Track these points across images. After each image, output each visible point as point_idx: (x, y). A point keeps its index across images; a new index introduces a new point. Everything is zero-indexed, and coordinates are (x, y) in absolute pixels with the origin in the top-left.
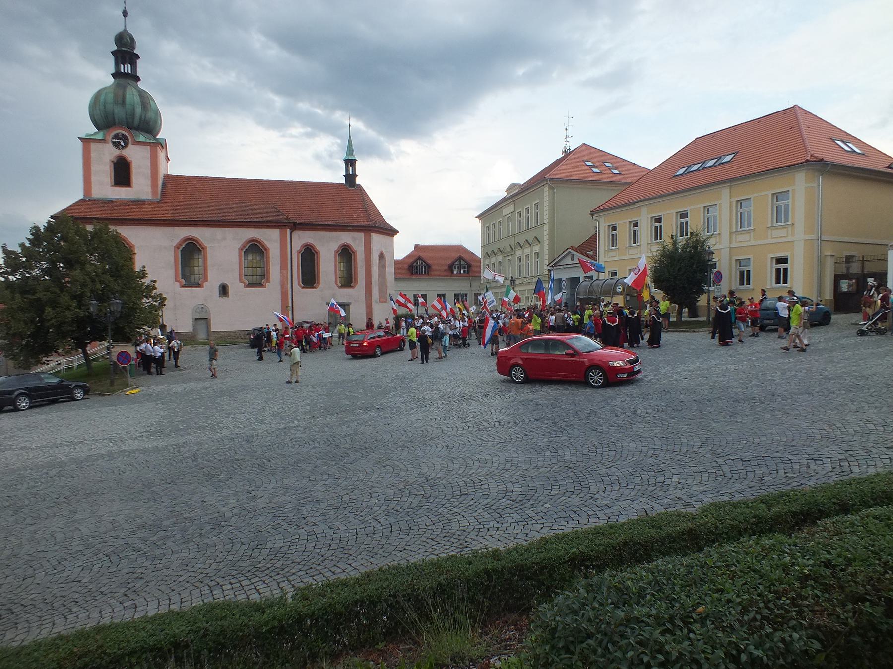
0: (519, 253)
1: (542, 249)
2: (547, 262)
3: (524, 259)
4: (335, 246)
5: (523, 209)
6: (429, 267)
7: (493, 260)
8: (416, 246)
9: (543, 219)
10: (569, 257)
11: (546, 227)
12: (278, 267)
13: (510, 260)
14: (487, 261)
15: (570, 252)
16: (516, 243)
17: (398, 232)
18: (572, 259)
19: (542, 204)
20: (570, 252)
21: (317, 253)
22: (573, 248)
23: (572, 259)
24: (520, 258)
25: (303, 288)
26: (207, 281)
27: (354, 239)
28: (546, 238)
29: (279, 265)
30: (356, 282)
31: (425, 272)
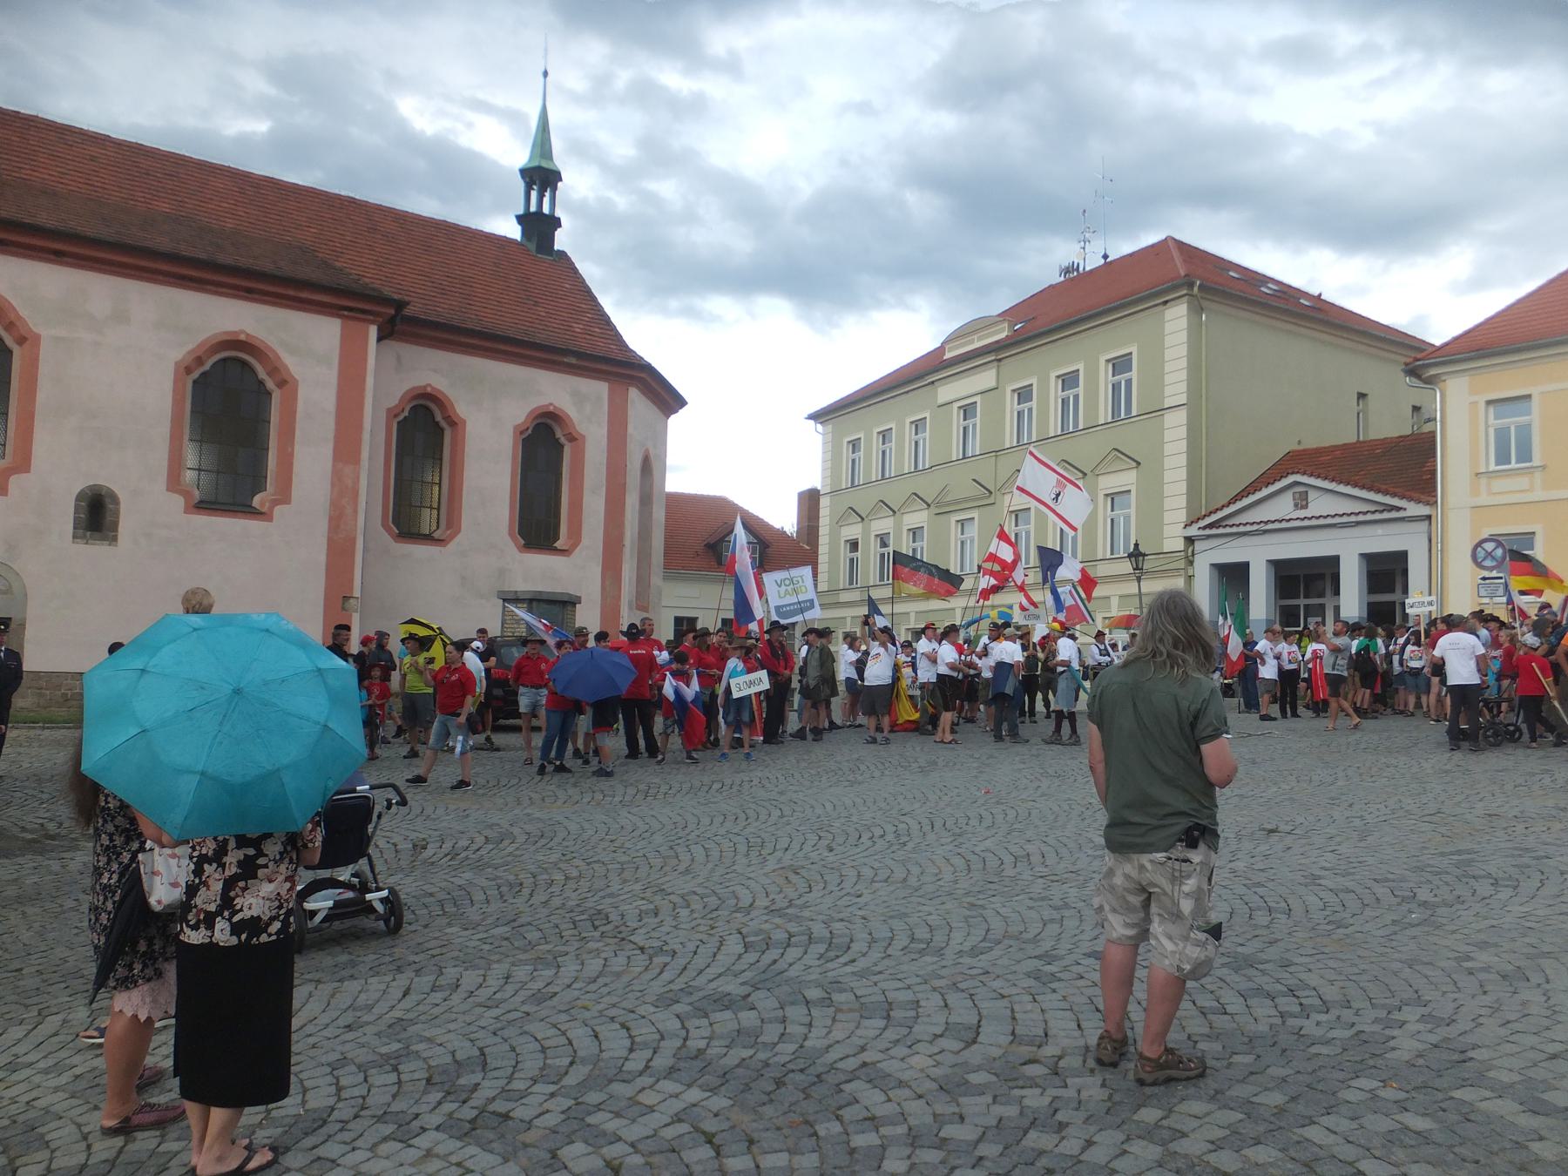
4: (517, 413)
12: (327, 451)
18: (1302, 502)
21: (455, 423)
23: (1302, 502)
26: (27, 470)
29: (330, 446)
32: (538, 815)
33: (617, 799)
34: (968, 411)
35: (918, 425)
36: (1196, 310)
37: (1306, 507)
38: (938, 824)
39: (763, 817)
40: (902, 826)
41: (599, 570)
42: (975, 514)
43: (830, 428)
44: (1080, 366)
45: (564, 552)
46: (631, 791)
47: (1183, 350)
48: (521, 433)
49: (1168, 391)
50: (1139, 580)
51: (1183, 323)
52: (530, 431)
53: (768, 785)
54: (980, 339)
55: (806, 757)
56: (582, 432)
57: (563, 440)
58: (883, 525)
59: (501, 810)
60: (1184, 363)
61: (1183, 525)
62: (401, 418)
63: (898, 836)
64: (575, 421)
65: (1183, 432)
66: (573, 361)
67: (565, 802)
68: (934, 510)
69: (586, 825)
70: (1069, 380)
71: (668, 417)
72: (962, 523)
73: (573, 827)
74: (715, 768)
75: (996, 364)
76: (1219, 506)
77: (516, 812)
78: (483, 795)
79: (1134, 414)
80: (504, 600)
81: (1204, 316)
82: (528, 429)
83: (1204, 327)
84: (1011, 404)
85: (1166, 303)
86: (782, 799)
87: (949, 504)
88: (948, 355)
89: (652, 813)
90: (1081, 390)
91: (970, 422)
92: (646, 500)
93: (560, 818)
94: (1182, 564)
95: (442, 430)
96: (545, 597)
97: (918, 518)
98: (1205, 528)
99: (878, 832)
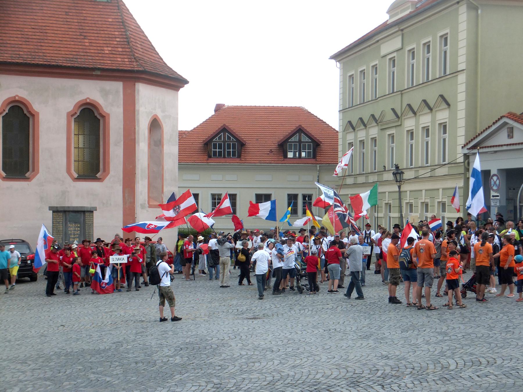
0: (409, 123)
1: (453, 117)
2: (461, 141)
3: (419, 135)
5: (418, 45)
6: (242, 144)
7: (362, 135)
8: (219, 108)
9: (455, 62)
10: (504, 133)
11: (462, 78)
13: (392, 136)
14: (350, 137)
15: (506, 124)
16: (404, 105)
17: (185, 82)
18: (510, 136)
19: (455, 31)
20: (506, 124)
21: (34, 115)
22: (512, 116)
23: (510, 136)
24: (411, 133)
25: (4, 179)
27: (105, 93)
28: (462, 97)
30: (106, 171)
31: (234, 155)
36: (473, 8)
37: (512, 137)
41: (121, 188)
48: (72, 116)
56: (108, 113)
62: (4, 114)
64: (103, 106)
66: (99, 73)
71: (178, 90)
80: (54, 212)
81: (479, 12)
82: (76, 113)
96: (71, 209)
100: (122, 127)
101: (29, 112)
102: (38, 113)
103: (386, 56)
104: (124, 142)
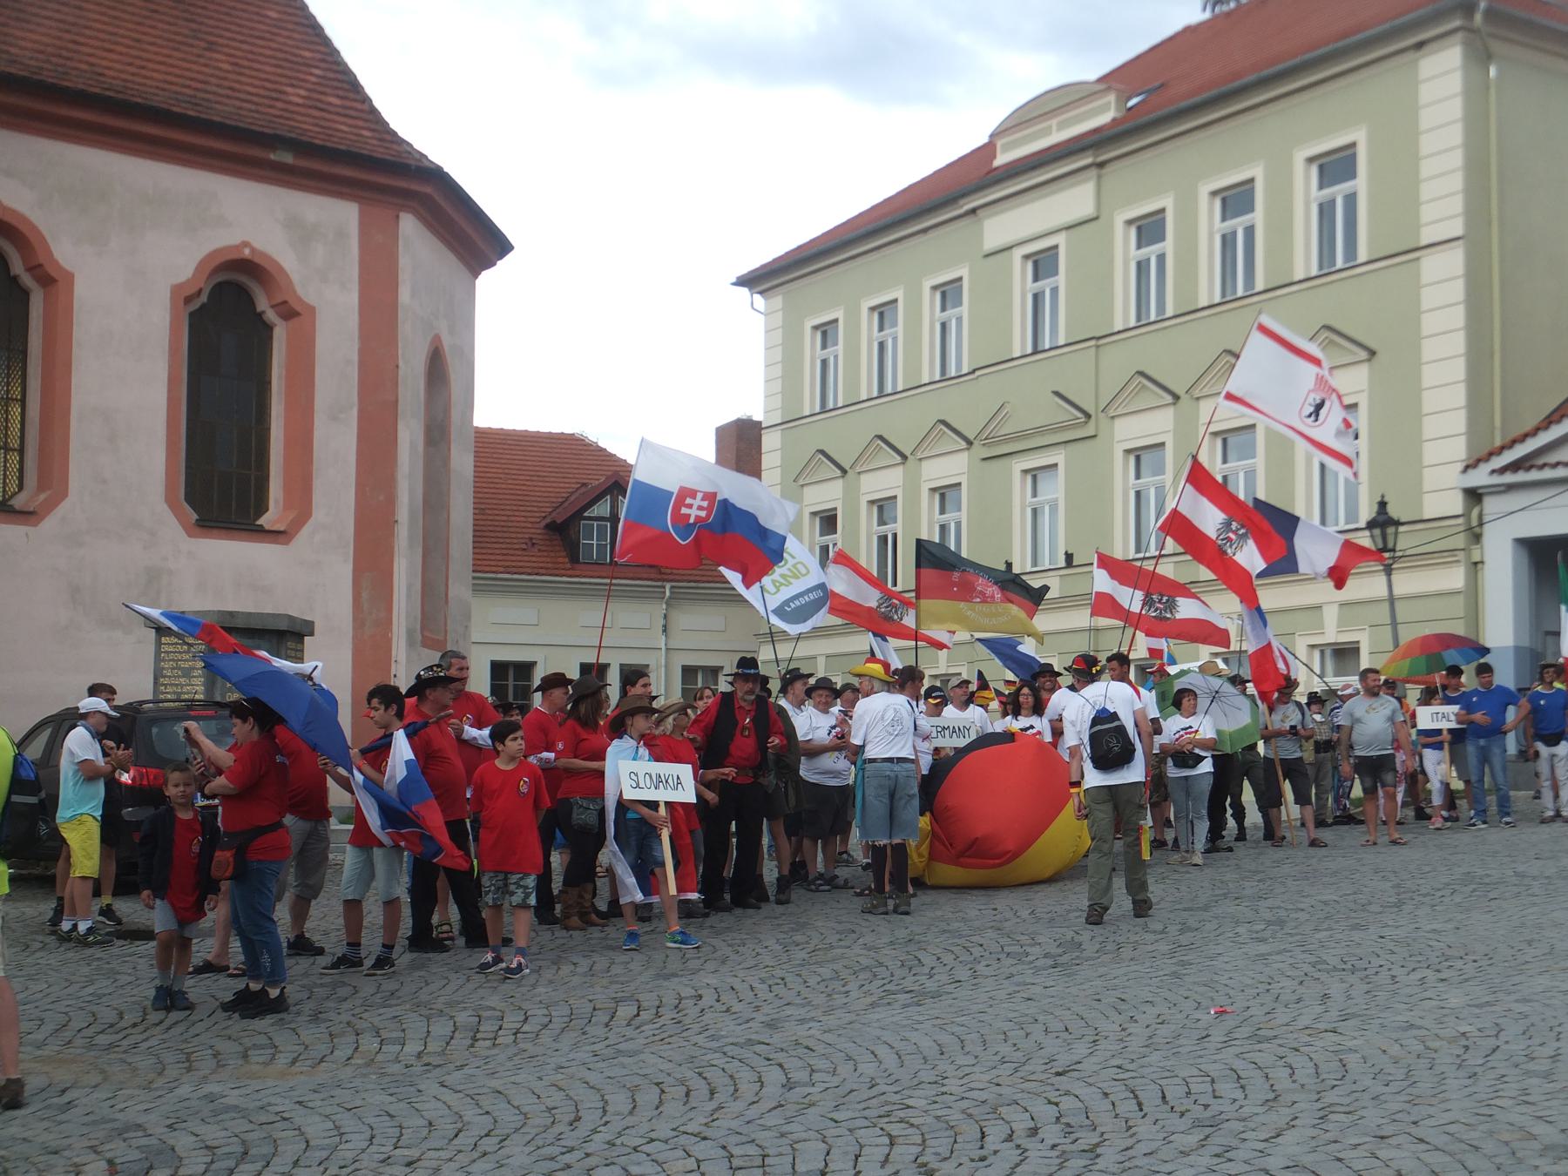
21: (51, 279)
27: (303, 235)
30: (302, 507)
32: (233, 1098)
33: (412, 1048)
34: (1043, 263)
35: (948, 293)
36: (1479, 56)
38: (1150, 1096)
39: (747, 1088)
40: (1067, 1103)
41: (346, 570)
42: (1058, 457)
43: (778, 301)
44: (1257, 172)
45: (278, 536)
46: (441, 1028)
47: (1456, 135)
48: (188, 300)
49: (1427, 213)
50: (1388, 571)
51: (1455, 83)
52: (204, 298)
53: (737, 1007)
54: (1061, 127)
55: (799, 938)
56: (312, 303)
57: (271, 316)
58: (884, 481)
59: (148, 1087)
60: (1457, 159)
61: (1460, 466)
63: (1069, 1129)
64: (295, 278)
65: (1457, 290)
66: (287, 158)
67: (294, 1062)
68: (980, 451)
69: (347, 1122)
70: (1236, 200)
71: (476, 275)
72: (1034, 474)
73: (316, 1128)
74: (616, 970)
75: (1094, 172)
76: (1528, 427)
77: (184, 1090)
78: (111, 1046)
79: (1362, 256)
81: (1493, 72)
82: (200, 291)
83: (1493, 91)
84: (1124, 247)
85: (1420, 45)
86: (776, 1039)
87: (1008, 439)
88: (1001, 159)
89: (495, 1084)
90: (1258, 217)
91: (1046, 284)
92: (437, 433)
93: (285, 1105)
94: (1460, 541)
95: (25, 294)
96: (240, 624)
97: (950, 467)
98: (1502, 471)
99: (1021, 1123)
100: (355, 358)
101: (36, 269)
102: (70, 277)
103: (1010, 248)
104: (361, 412)
